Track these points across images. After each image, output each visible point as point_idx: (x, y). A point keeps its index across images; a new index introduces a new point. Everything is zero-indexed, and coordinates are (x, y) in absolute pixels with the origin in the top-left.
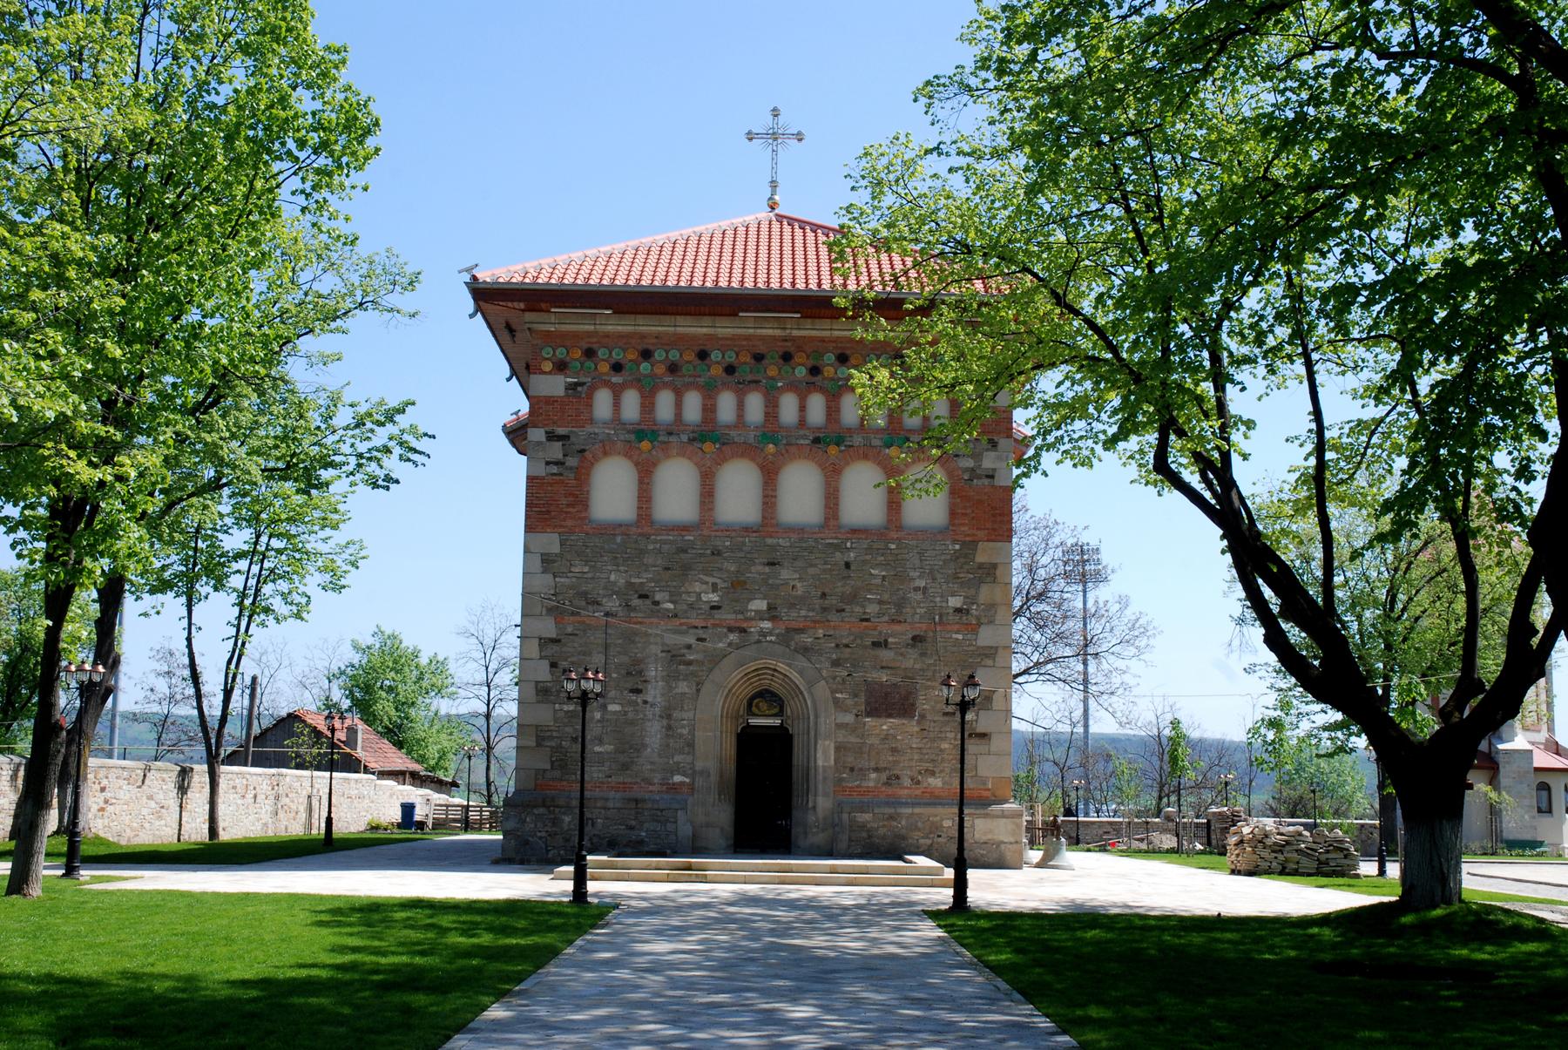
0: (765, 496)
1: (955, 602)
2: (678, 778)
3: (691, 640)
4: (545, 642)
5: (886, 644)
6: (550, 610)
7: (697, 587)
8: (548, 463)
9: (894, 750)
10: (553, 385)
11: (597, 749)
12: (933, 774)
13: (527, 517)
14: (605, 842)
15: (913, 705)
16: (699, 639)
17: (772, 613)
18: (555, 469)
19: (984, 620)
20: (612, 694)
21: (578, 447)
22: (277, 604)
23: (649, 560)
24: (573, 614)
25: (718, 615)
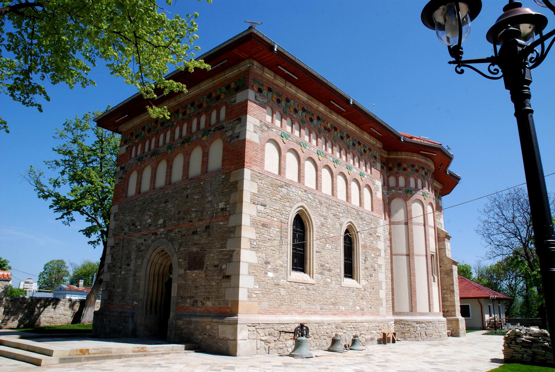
1: (221, 205)
2: (135, 303)
9: (196, 287)
15: (203, 262)
17: (164, 225)
19: (232, 212)
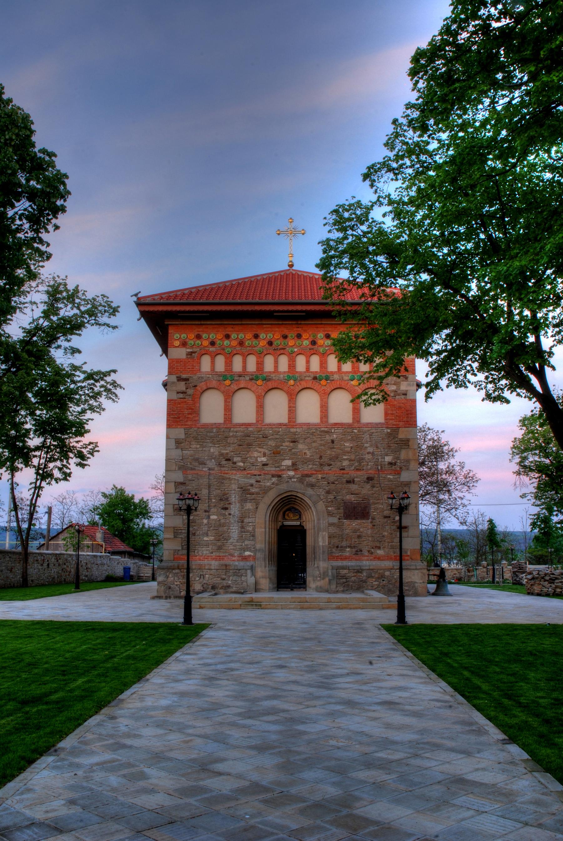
0: (290, 407)
1: (388, 459)
2: (247, 553)
3: (253, 481)
4: (178, 484)
5: (354, 481)
6: (180, 468)
7: (256, 454)
8: (178, 393)
10: (179, 353)
11: (205, 539)
12: (379, 548)
13: (168, 420)
14: (210, 587)
15: (368, 513)
16: (257, 481)
18: (181, 396)
20: (213, 510)
21: (193, 384)
22: (57, 474)
23: (230, 440)
24: (192, 469)
25: (266, 468)
